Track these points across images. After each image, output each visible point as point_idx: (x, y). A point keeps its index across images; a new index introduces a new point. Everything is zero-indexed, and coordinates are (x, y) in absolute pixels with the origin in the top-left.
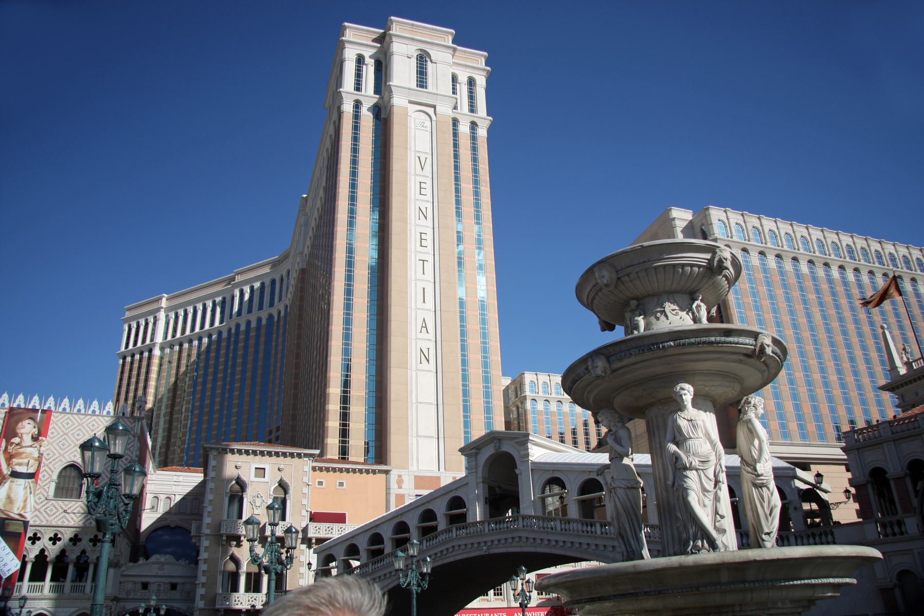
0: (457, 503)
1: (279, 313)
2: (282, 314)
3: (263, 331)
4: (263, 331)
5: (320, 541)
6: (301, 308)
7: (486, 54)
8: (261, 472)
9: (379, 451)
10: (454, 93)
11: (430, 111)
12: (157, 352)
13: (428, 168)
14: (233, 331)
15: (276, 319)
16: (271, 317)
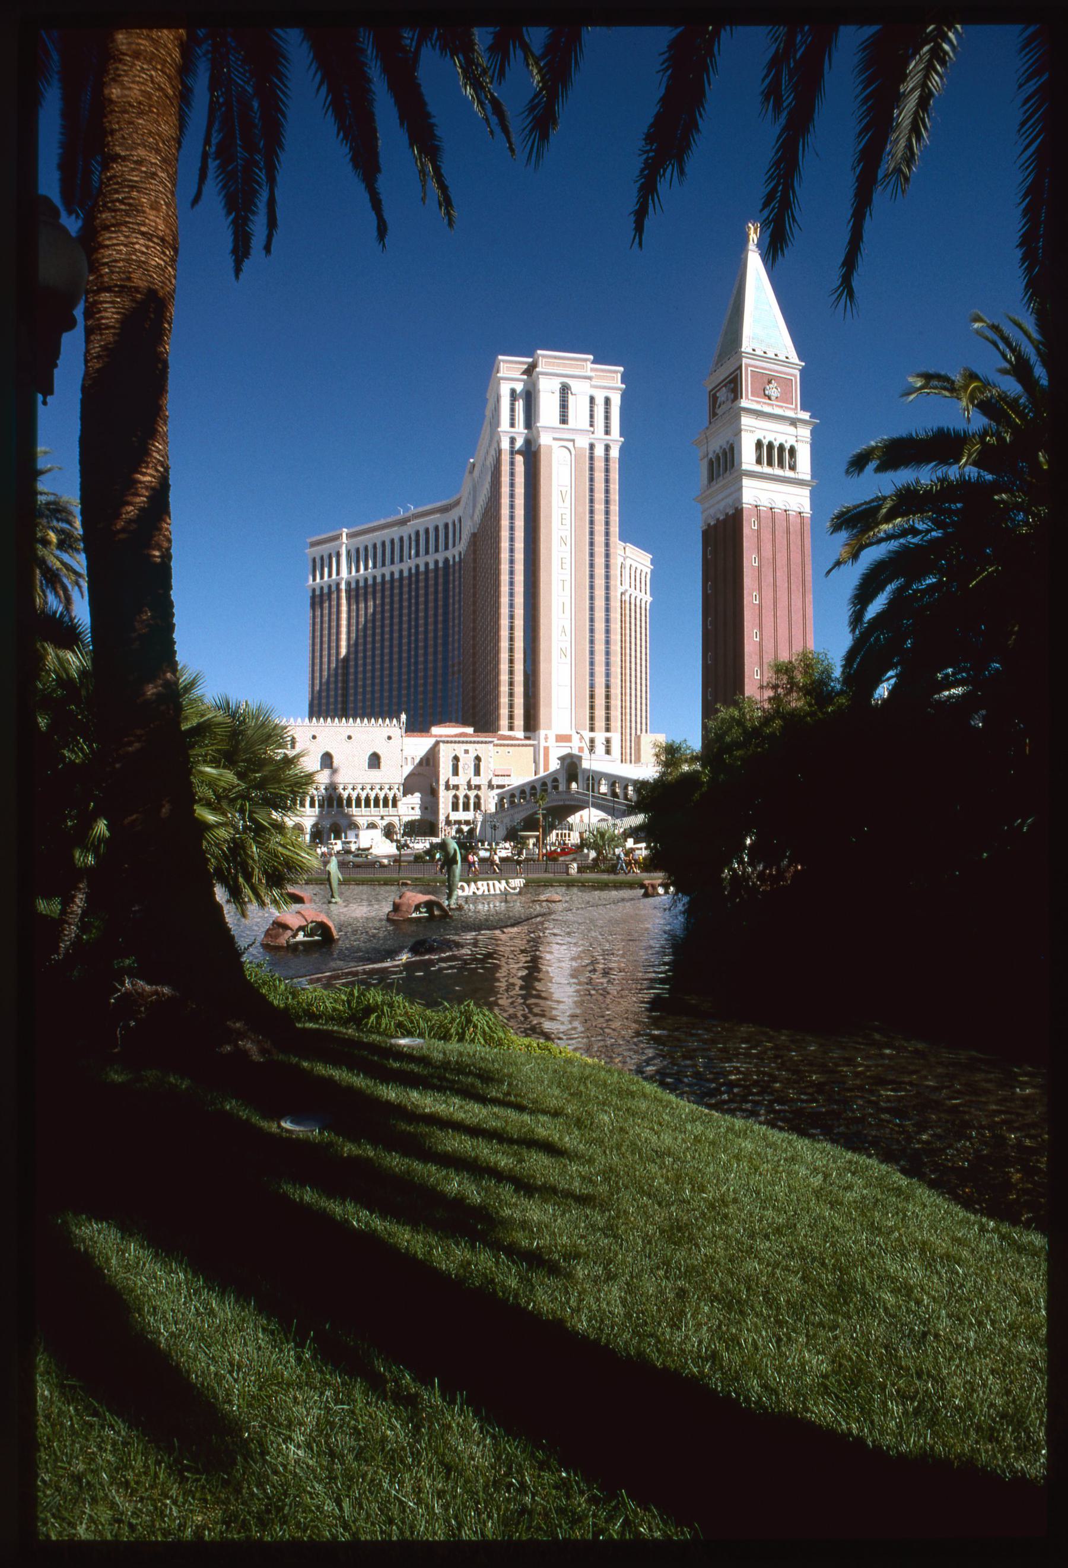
0: (555, 780)
1: (454, 557)
2: (457, 559)
3: (441, 573)
4: (441, 573)
5: (499, 787)
6: (475, 552)
7: (621, 369)
8: (466, 752)
9: (531, 724)
10: (592, 425)
11: (570, 445)
12: (343, 586)
13: (568, 500)
14: (413, 571)
15: (451, 563)
16: (446, 560)
